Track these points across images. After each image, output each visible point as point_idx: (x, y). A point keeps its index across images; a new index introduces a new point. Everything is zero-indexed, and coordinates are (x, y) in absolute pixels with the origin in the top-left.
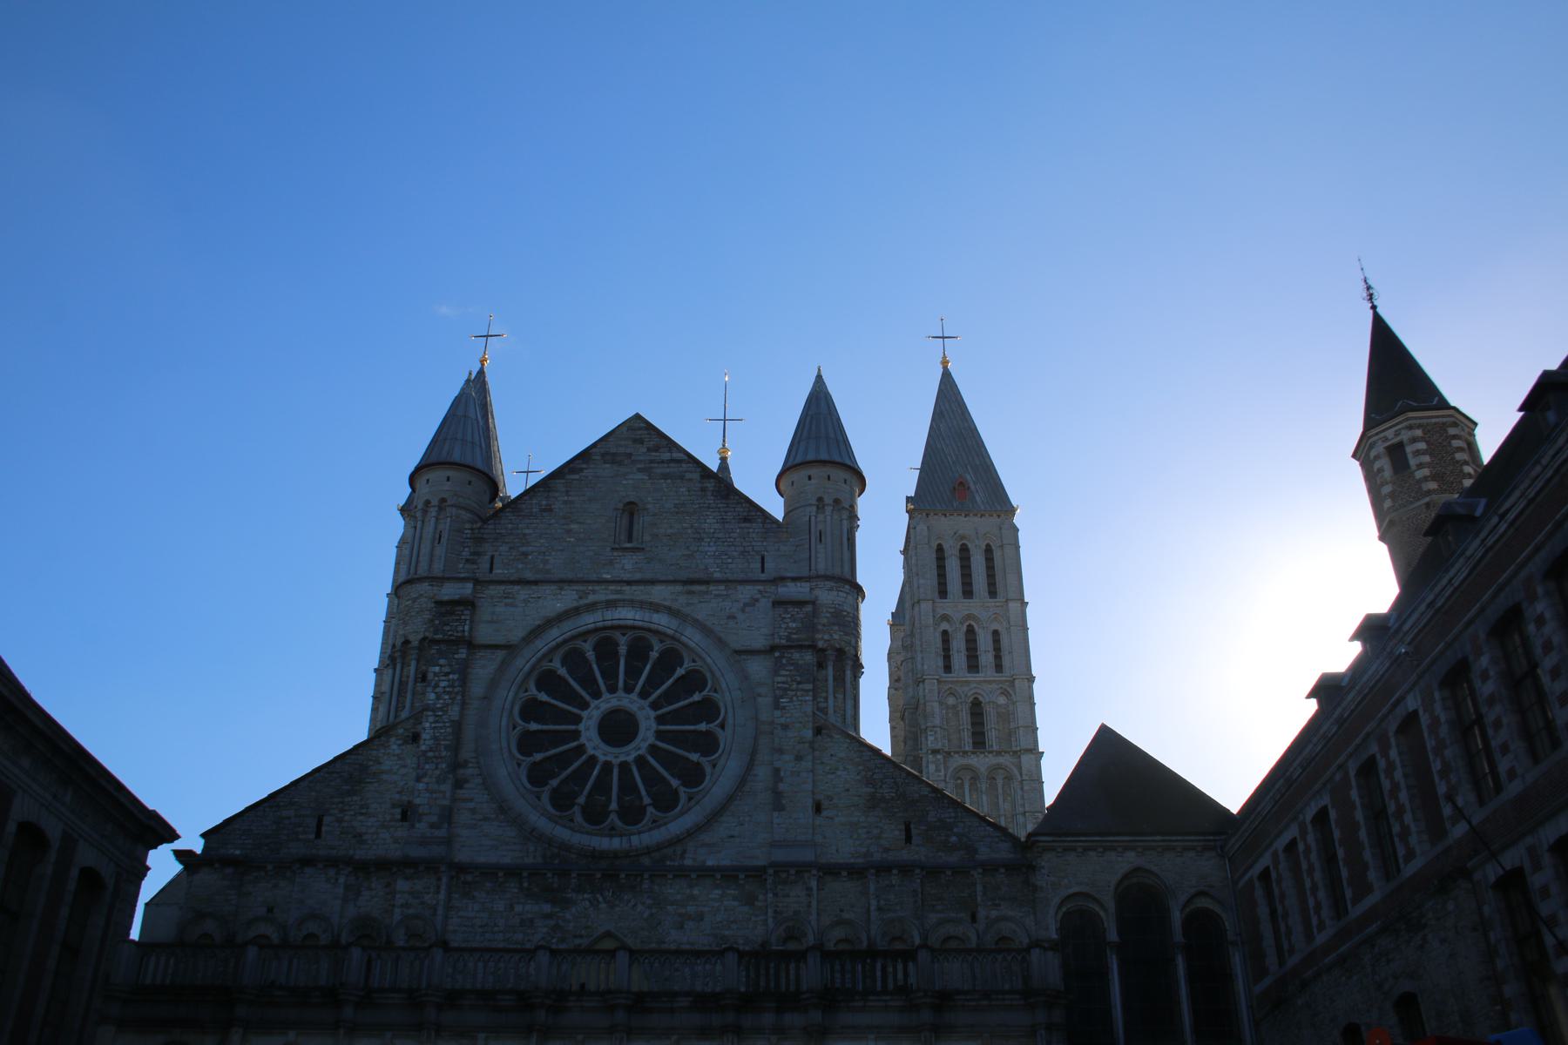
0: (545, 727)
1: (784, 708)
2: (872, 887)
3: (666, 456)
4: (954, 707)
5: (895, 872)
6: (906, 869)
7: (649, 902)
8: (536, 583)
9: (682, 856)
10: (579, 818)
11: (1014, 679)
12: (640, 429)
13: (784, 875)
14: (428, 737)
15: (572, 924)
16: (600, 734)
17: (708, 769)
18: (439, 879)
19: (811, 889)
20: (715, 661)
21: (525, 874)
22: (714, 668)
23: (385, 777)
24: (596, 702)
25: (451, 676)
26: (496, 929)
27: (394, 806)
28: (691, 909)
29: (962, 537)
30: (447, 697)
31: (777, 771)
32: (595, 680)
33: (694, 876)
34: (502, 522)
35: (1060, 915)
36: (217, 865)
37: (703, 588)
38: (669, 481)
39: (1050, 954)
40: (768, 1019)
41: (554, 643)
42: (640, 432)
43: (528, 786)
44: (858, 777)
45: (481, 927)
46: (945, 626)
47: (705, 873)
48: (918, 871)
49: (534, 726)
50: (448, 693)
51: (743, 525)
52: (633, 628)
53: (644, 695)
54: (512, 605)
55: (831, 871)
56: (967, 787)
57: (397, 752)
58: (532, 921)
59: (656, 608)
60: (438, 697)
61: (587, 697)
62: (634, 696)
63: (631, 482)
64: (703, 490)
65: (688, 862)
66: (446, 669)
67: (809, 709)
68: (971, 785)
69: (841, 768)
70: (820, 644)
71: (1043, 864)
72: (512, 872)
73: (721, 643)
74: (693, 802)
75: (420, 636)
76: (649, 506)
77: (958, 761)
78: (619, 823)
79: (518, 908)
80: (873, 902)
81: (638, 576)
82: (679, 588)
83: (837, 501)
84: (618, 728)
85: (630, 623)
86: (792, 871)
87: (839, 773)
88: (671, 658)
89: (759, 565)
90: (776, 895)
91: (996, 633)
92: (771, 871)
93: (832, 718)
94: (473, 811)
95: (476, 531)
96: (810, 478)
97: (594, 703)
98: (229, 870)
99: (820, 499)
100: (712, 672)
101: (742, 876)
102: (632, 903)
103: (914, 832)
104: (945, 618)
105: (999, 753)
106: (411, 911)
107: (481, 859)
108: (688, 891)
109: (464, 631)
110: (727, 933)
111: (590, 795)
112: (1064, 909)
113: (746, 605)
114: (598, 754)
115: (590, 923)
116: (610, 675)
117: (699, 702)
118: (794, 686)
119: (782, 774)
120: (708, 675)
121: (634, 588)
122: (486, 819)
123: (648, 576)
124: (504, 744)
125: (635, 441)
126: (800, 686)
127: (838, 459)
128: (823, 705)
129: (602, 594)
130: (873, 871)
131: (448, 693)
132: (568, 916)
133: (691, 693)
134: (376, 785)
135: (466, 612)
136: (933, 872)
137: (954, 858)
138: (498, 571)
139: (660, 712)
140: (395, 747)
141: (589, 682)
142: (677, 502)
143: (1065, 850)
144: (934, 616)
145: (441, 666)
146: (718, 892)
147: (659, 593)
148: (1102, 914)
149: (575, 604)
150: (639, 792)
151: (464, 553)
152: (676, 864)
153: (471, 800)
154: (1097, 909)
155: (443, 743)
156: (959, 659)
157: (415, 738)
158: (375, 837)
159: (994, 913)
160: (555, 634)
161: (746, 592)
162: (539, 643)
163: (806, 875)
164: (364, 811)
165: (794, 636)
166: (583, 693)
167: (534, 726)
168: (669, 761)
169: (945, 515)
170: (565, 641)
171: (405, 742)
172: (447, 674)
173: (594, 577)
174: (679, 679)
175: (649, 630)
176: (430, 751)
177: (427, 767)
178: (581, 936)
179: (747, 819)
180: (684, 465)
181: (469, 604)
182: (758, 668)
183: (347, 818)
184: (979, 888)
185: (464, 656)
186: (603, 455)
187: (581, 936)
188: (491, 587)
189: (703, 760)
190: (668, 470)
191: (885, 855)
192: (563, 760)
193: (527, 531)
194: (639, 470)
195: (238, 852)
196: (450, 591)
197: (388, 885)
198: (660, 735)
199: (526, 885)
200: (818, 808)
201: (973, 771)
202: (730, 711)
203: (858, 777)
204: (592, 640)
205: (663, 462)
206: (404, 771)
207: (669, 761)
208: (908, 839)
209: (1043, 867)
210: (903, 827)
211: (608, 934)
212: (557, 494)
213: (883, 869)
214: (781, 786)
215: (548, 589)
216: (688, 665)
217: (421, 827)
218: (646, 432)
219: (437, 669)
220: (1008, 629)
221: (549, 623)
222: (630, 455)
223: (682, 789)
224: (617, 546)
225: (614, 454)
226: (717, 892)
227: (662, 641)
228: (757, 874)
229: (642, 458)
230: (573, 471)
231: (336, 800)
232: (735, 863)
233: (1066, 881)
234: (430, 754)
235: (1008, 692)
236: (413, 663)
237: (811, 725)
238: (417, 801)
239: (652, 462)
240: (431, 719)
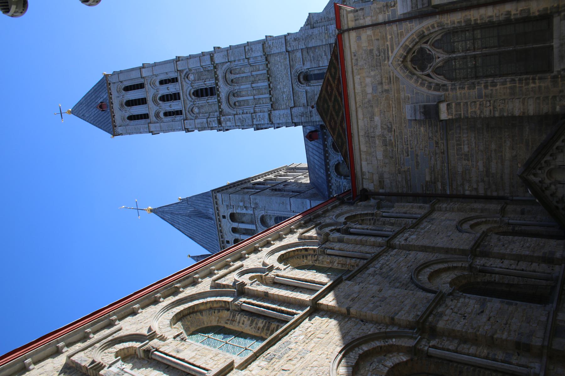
4: (199, 108)
11: (177, 70)
29: (122, 105)
46: (161, 115)
56: (241, 99)
68: (238, 96)
77: (224, 106)
91: (162, 82)
104: (157, 115)
105: (217, 79)
144: (157, 123)
156: (175, 106)
169: (114, 116)
201: (229, 94)
220: (156, 76)
235: (186, 74)
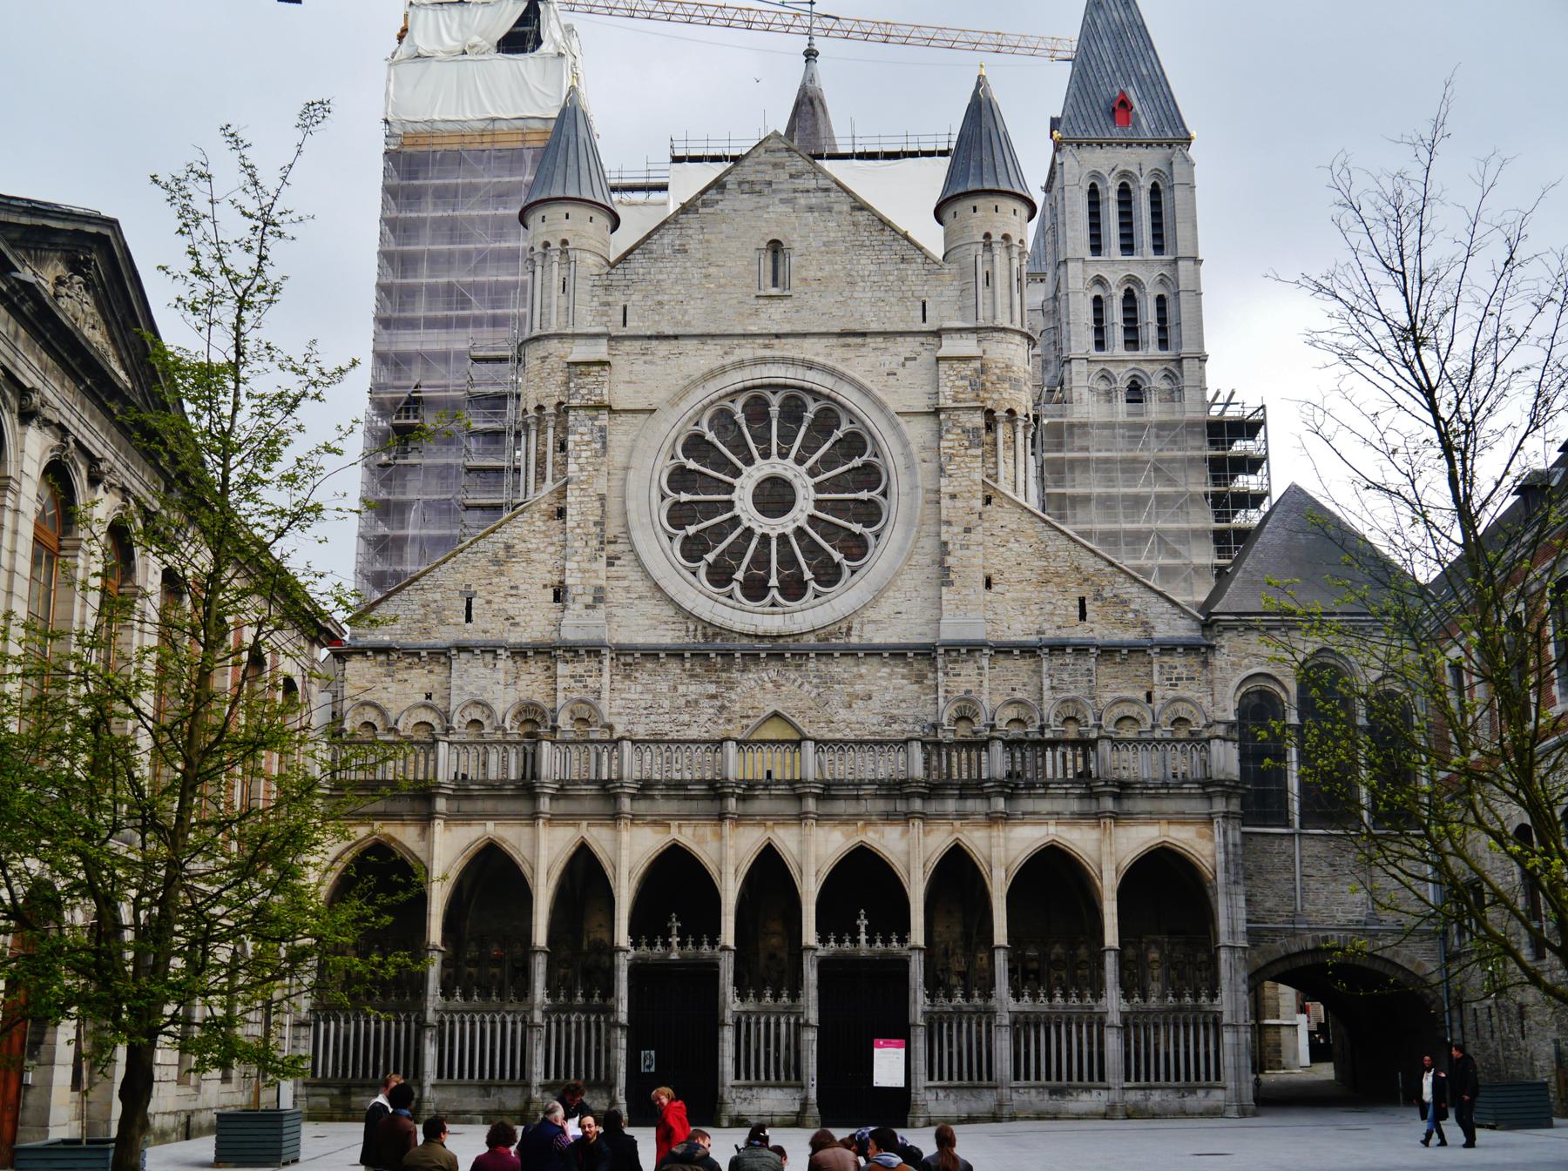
0: (696, 498)
1: (950, 476)
2: (1045, 665)
3: (812, 184)
5: (1069, 650)
6: (1081, 649)
7: (815, 681)
8: (676, 337)
9: (848, 634)
10: (738, 593)
12: (779, 150)
13: (954, 654)
14: (575, 512)
15: (738, 705)
16: (755, 504)
17: (871, 540)
18: (600, 662)
19: (983, 668)
20: (875, 423)
21: (687, 655)
22: (875, 431)
23: (534, 556)
24: (749, 469)
25: (594, 445)
26: (661, 711)
27: (545, 586)
28: (859, 688)
30: (590, 469)
31: (945, 544)
32: (746, 444)
33: (861, 654)
34: (632, 265)
35: (1239, 694)
36: (370, 653)
37: (859, 340)
38: (816, 214)
39: (1230, 744)
40: (951, 805)
41: (700, 406)
42: (778, 154)
43: (683, 561)
44: (1030, 550)
45: (645, 709)
47: (874, 652)
48: (1092, 650)
49: (684, 497)
50: (592, 463)
51: (902, 266)
52: (785, 387)
53: (800, 461)
54: (651, 363)
55: (1003, 650)
57: (544, 528)
58: (696, 702)
59: (810, 366)
60: (581, 470)
61: (739, 464)
62: (790, 461)
63: (772, 215)
64: (855, 224)
65: (854, 640)
66: (586, 438)
67: (978, 476)
69: (1012, 540)
70: (989, 405)
71: (1223, 643)
72: (676, 654)
73: (881, 406)
74: (856, 577)
75: (555, 401)
76: (796, 245)
78: (779, 599)
79: (681, 689)
80: (1047, 682)
81: (786, 328)
82: (833, 341)
83: (1006, 237)
84: (775, 497)
85: (781, 381)
86: (963, 651)
87: (1010, 545)
88: (828, 418)
89: (921, 313)
90: (946, 674)
92: (941, 651)
93: (1004, 486)
94: (627, 590)
95: (605, 277)
96: (975, 210)
97: (746, 470)
98: (382, 658)
99: (987, 236)
100: (873, 438)
101: (910, 654)
102: (799, 681)
103: (1088, 608)
106: (575, 695)
107: (640, 639)
108: (855, 669)
109: (602, 394)
110: (895, 712)
111: (748, 568)
112: (1243, 689)
113: (906, 359)
114: (754, 525)
115: (756, 704)
116: (762, 439)
117: (858, 468)
118: (963, 452)
119: (950, 547)
120: (867, 438)
121: (783, 341)
122: (640, 598)
123: (799, 328)
124: (656, 519)
125: (775, 165)
126: (969, 452)
127: (1004, 187)
128: (991, 472)
129: (747, 351)
130: (1047, 650)
131: (592, 463)
132: (734, 697)
133: (851, 458)
134: (524, 564)
135: (603, 373)
136: (1108, 652)
137: (1131, 635)
138: (634, 326)
139: (818, 479)
140: (540, 523)
141: (740, 447)
142: (825, 239)
143: (1249, 629)
145: (582, 434)
146: (887, 670)
147: (812, 350)
148: (1283, 695)
149: (720, 362)
150: (799, 565)
151: (593, 304)
152: (842, 641)
153: (624, 578)
154: (1278, 689)
155: (591, 518)
157: (561, 513)
158: (528, 618)
159: (1171, 694)
160: (699, 397)
161: (907, 346)
162: (684, 406)
163: (977, 654)
164: (513, 592)
165: (961, 396)
166: (734, 459)
167: (684, 497)
168: (829, 531)
170: (712, 403)
171: (551, 518)
172: (588, 443)
173: (739, 330)
174: (836, 442)
175: (802, 389)
176: (579, 526)
177: (576, 544)
178: (748, 717)
179: (915, 594)
180: (832, 195)
181: (603, 363)
182: (918, 431)
183: (496, 600)
184: (1156, 667)
185: (605, 423)
186: (740, 184)
187: (748, 717)
188: (627, 343)
189: (867, 531)
190: (814, 201)
191: (1058, 632)
192: (719, 532)
193: (661, 277)
194: (782, 201)
195: (387, 638)
196: (581, 351)
197: (548, 668)
198: (819, 504)
199: (688, 665)
200: (988, 583)
202: (893, 478)
203: (1030, 550)
204: (741, 401)
205: (808, 191)
206: (552, 549)
207: (829, 531)
208: (1083, 616)
209: (1223, 647)
210: (1077, 603)
211: (776, 715)
212: (690, 232)
213: (1057, 648)
214: (950, 561)
215: (690, 345)
216: (845, 427)
217: (575, 608)
218: (786, 154)
219: (577, 438)
221: (694, 384)
222: (770, 183)
223: (845, 562)
224: (762, 293)
225: (753, 183)
226: (884, 670)
227: (816, 400)
228: (927, 653)
229: (784, 186)
230: (704, 204)
231: (483, 582)
232: (903, 641)
233: (1246, 661)
234: (578, 531)
236: (550, 432)
237: (980, 495)
238: (568, 581)
239: (795, 191)
240: (577, 493)
